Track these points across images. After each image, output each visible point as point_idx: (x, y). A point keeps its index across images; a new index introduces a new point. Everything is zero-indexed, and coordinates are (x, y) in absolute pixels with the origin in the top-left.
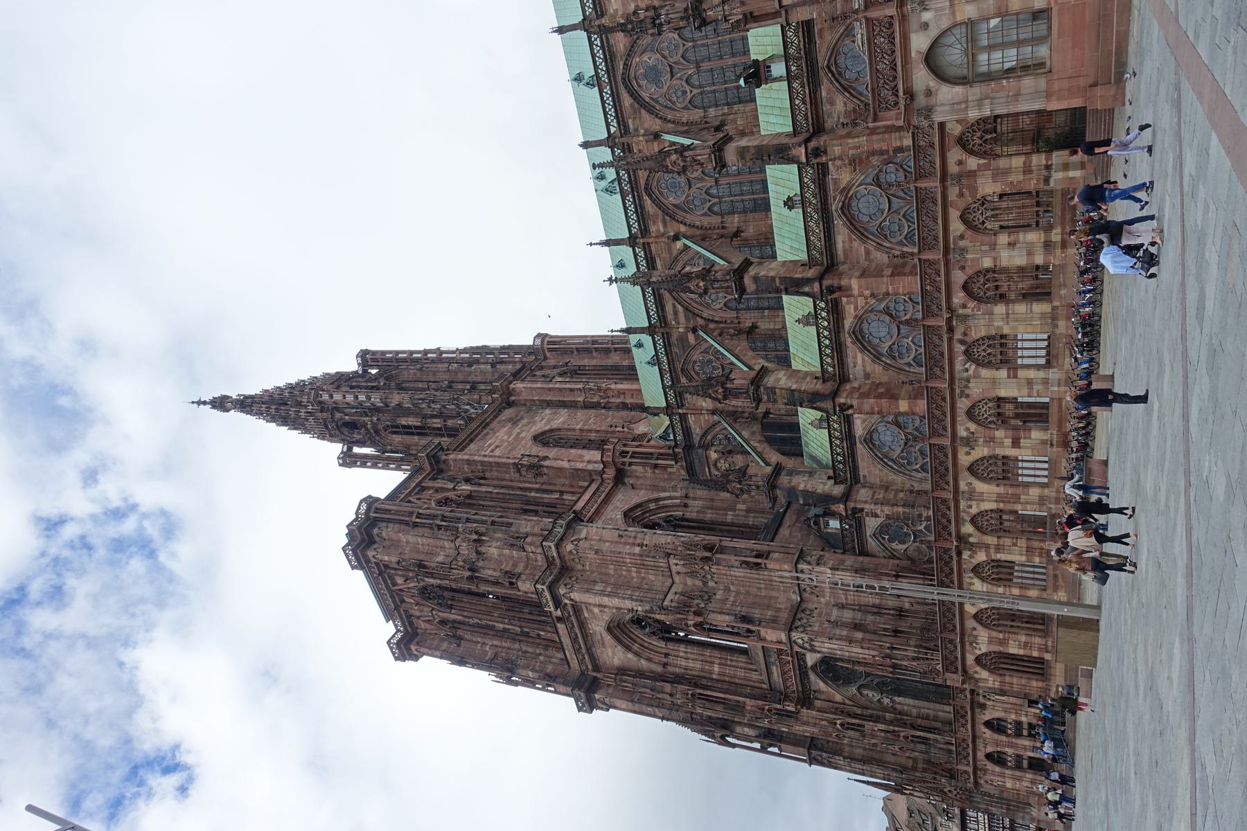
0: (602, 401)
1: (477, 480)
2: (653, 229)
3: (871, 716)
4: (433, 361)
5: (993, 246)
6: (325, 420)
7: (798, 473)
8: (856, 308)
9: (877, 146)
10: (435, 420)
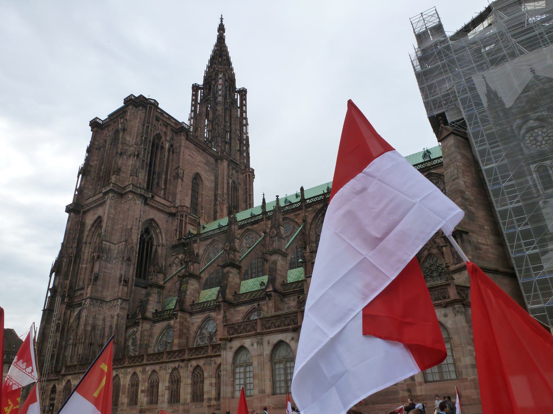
0: (218, 202)
3: (63, 335)
4: (241, 122)
5: (211, 377)
6: (211, 76)
7: (159, 296)
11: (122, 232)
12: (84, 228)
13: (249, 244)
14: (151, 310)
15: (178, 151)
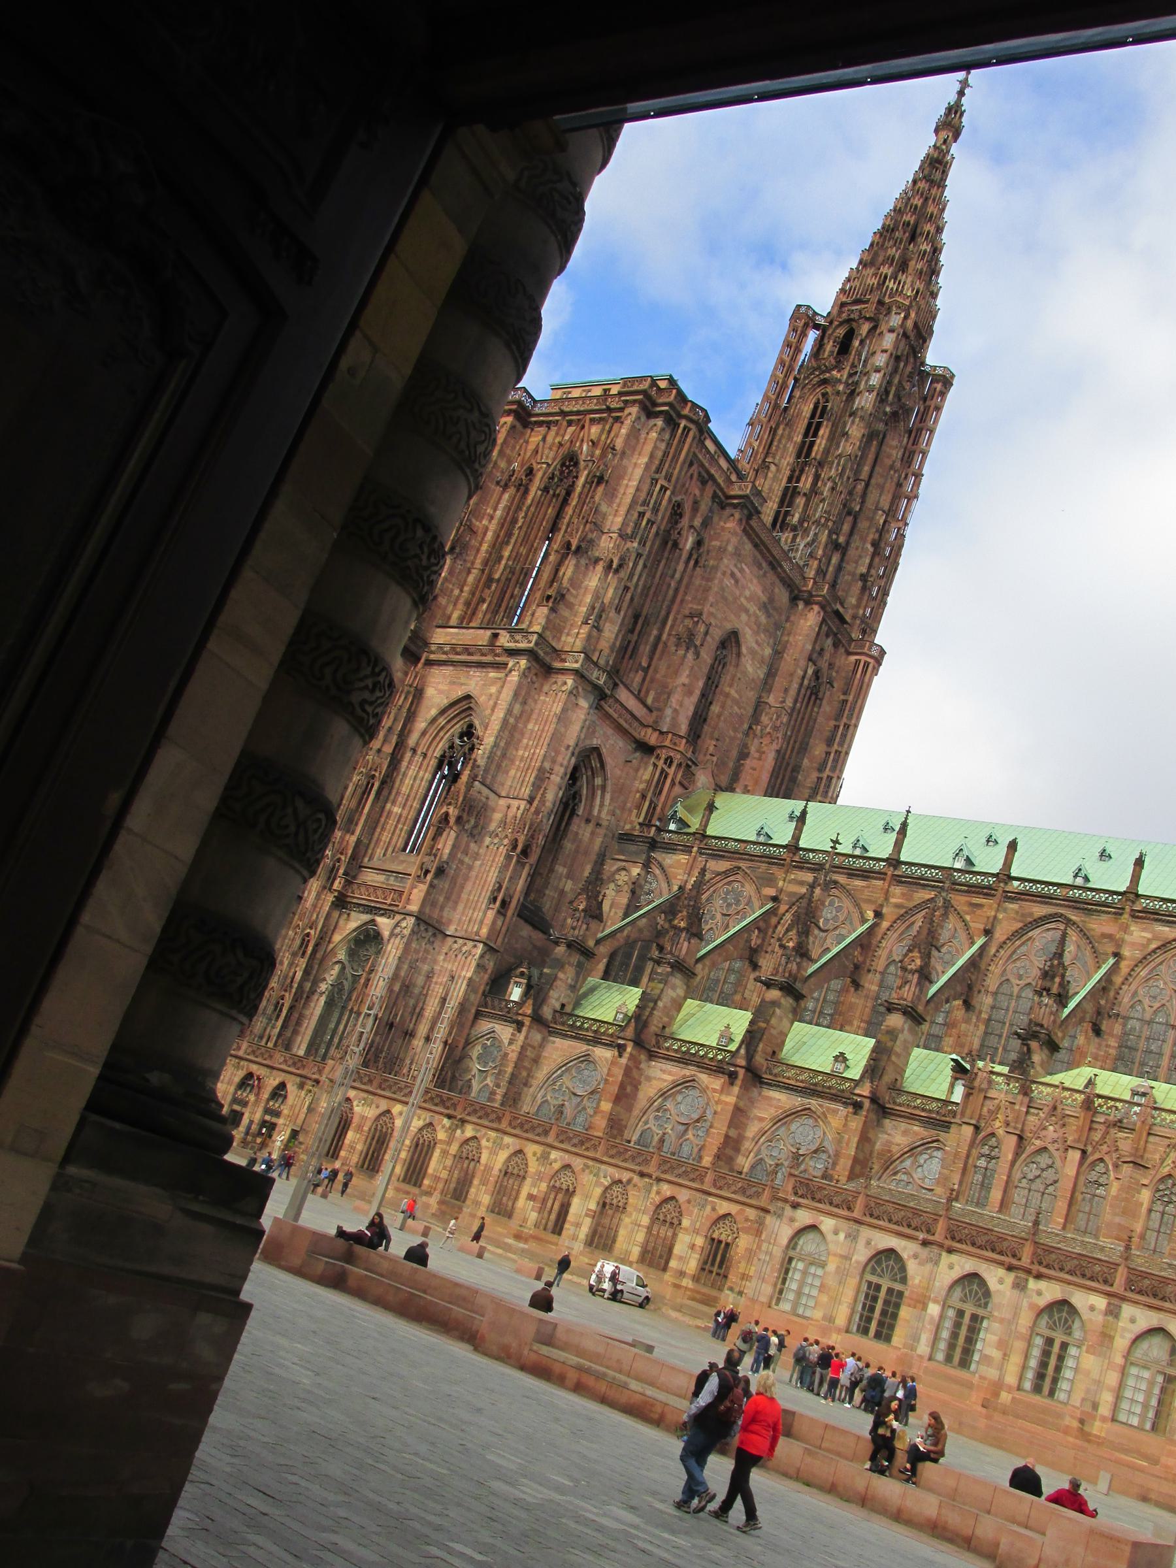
1: (695, 556)
2: (897, 890)
3: (312, 967)
4: (899, 485)
5: (696, 1232)
7: (578, 974)
8: (714, 1090)
9: (842, 1161)
10: (810, 480)
14: (553, 1001)
15: (711, 562)
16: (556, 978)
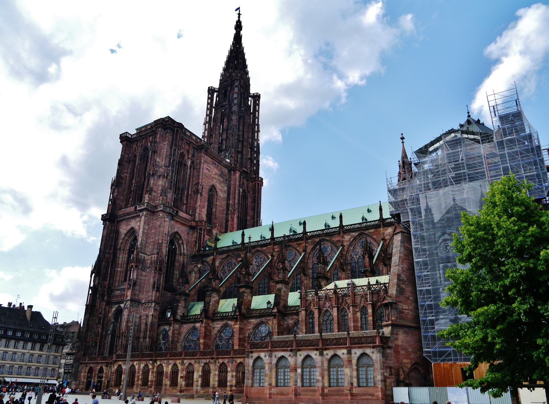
1: (192, 166)
2: (276, 247)
3: (104, 327)
4: (253, 129)
5: (232, 371)
7: (186, 303)
10: (225, 135)
11: (154, 245)
12: (118, 235)
13: (258, 263)
16: (178, 306)
